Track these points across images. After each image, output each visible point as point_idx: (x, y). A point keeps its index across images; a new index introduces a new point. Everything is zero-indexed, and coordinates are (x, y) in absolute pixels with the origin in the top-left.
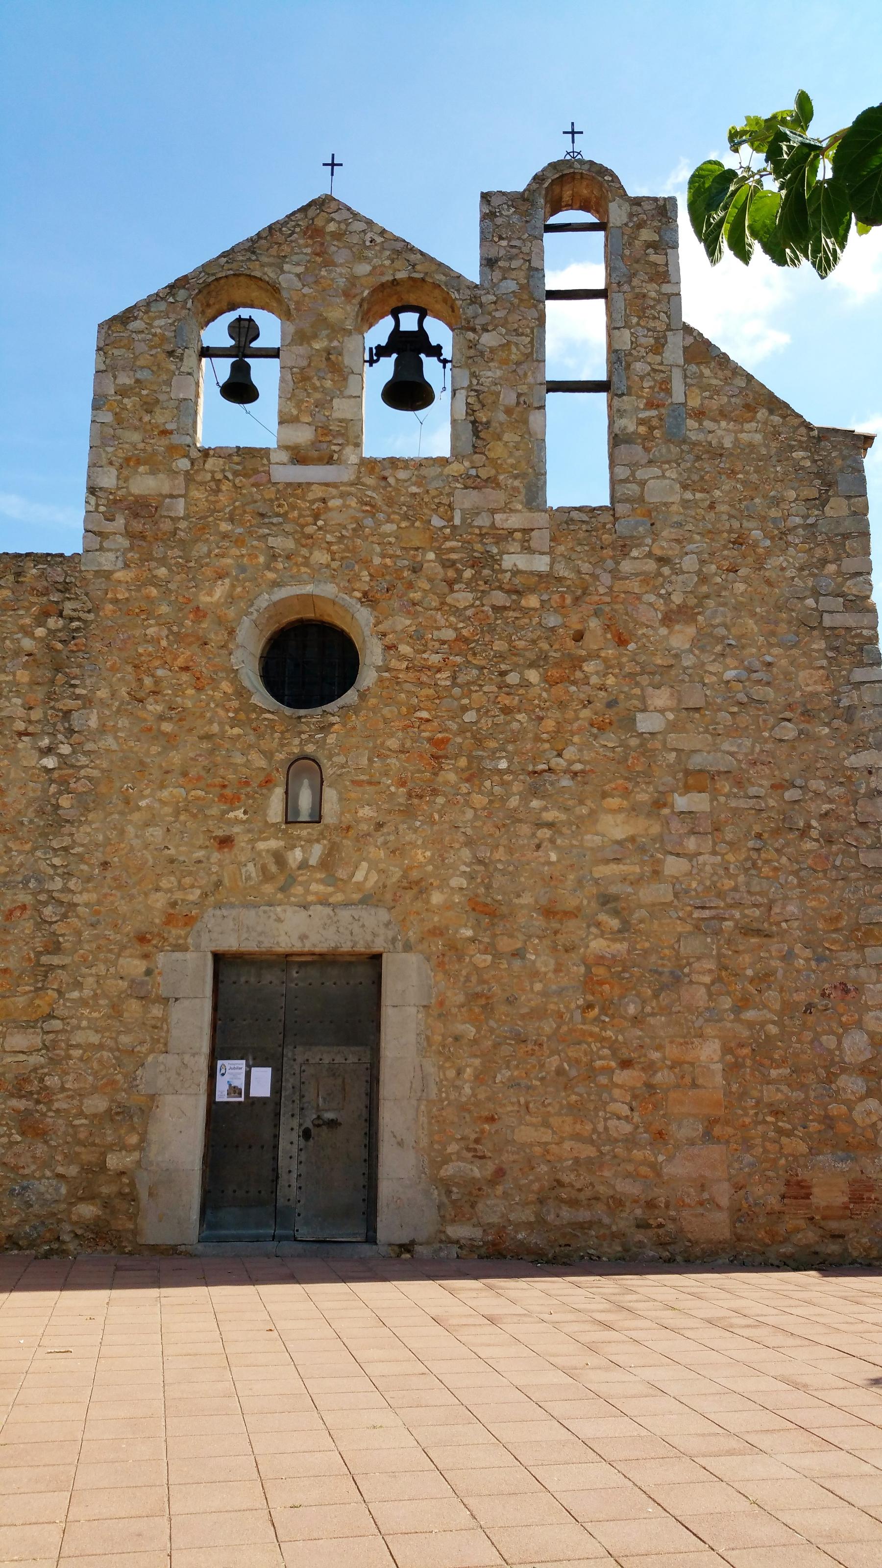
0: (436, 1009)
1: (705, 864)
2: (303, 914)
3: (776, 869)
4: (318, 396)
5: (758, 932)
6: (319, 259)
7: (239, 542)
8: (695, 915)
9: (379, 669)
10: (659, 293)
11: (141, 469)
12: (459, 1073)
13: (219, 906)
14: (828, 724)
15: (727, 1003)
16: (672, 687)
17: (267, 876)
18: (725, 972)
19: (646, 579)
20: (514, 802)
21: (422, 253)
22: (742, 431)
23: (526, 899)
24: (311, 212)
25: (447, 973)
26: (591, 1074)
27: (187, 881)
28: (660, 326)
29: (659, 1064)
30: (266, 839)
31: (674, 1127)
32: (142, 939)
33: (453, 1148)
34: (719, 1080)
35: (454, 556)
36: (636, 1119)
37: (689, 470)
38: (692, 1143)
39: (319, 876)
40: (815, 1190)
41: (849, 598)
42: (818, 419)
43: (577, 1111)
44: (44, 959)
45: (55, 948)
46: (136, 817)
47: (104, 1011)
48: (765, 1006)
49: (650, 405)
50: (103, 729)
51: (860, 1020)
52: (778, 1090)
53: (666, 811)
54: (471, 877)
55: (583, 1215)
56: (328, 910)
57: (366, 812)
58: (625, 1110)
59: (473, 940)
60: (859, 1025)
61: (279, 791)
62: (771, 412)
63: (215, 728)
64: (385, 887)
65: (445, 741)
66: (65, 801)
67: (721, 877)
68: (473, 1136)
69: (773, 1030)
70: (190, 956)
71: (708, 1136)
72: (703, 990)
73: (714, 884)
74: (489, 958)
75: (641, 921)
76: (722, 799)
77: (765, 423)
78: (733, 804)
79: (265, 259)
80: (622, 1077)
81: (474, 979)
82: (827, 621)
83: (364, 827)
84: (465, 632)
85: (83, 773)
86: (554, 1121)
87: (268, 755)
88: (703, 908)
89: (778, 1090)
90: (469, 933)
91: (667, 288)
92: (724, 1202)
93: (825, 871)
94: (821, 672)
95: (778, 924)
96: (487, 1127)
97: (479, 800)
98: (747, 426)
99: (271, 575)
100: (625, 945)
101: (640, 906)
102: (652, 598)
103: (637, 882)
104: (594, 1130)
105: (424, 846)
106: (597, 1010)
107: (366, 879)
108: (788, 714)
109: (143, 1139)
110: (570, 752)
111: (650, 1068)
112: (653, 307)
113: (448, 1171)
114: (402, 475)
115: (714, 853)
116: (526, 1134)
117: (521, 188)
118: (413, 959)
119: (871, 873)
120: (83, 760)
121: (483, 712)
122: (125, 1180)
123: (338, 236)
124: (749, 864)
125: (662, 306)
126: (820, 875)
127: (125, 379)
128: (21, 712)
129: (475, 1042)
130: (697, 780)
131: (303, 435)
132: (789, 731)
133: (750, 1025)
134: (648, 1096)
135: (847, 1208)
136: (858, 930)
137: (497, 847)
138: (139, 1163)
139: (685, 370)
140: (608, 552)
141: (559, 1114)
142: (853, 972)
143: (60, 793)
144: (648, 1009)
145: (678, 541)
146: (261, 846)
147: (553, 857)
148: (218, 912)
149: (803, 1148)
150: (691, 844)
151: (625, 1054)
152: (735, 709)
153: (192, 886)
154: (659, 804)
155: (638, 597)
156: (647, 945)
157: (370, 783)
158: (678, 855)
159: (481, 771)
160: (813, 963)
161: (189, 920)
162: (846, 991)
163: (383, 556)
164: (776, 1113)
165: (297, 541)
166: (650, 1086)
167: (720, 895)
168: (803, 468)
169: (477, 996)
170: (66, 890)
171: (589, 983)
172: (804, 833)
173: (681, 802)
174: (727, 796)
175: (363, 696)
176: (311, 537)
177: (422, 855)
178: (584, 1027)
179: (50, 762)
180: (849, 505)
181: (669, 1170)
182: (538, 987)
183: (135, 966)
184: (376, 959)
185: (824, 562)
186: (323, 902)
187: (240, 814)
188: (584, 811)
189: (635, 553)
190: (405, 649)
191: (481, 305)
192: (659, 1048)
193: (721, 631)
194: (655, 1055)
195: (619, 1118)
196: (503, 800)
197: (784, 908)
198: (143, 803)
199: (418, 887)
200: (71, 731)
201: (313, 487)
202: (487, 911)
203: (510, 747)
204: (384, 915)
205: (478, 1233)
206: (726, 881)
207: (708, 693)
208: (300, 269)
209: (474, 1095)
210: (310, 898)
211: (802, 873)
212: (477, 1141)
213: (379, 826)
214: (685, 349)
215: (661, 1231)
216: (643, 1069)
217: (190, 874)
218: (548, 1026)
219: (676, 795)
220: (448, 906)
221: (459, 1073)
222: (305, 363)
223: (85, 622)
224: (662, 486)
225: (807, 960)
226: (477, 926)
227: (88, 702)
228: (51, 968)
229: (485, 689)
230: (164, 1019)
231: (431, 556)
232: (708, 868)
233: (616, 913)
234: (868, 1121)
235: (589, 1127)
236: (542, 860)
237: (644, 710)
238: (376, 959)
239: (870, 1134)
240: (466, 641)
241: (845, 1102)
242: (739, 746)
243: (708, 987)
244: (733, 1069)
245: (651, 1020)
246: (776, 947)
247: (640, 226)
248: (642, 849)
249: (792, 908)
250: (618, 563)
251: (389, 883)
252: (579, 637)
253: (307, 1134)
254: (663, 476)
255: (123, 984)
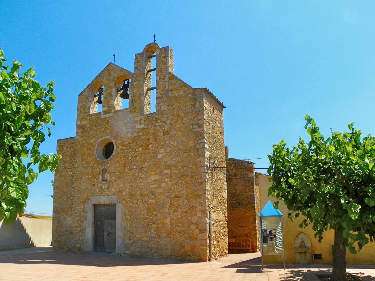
0: (124, 214)
1: (168, 184)
2: (104, 197)
3: (182, 184)
4: (108, 101)
5: (178, 197)
6: (109, 75)
7: (96, 131)
8: (167, 194)
9: (116, 151)
10: (165, 67)
11: (83, 120)
12: (127, 225)
13: (93, 196)
14: (193, 153)
15: (172, 211)
16: (164, 148)
17: (99, 191)
18: (172, 205)
19: (161, 126)
20: (136, 174)
21: (125, 69)
22: (180, 92)
23: (138, 193)
24: (108, 66)
25: (125, 207)
26: (148, 225)
27: (89, 192)
28: (165, 74)
29: (159, 223)
30: (99, 184)
31: (162, 235)
32: (83, 202)
33: (126, 238)
34: (170, 226)
35: (128, 127)
36: (155, 233)
37: (169, 103)
38: (165, 238)
39: (107, 190)
40: (185, 247)
41: (199, 125)
42: (194, 85)
43: (146, 232)
44: (72, 206)
45: (73, 204)
46: (82, 181)
47: (79, 214)
48: (178, 212)
49: (162, 90)
50: (78, 167)
51: (196, 214)
52: (180, 228)
53: (162, 174)
54: (129, 189)
55: (146, 250)
56: (108, 196)
57: (114, 178)
58: (153, 232)
59: (129, 201)
60: (196, 215)
61: (101, 175)
62: (185, 87)
63: (92, 165)
64: (116, 192)
65: (126, 163)
66: (73, 179)
67: (171, 186)
68: (129, 236)
69: (179, 216)
70: (89, 205)
71: (167, 237)
72: (167, 209)
73: (170, 188)
74: (132, 204)
75: (157, 196)
76: (172, 171)
77: (184, 90)
78: (174, 171)
79: (101, 77)
80: (153, 226)
81: (130, 208)
82: (194, 130)
83: (113, 181)
84: (129, 142)
85: (75, 175)
86: (142, 234)
87: (100, 169)
88: (168, 193)
89: (180, 228)
90: (129, 200)
91: (166, 66)
92: (170, 249)
93: (191, 184)
94: (193, 141)
95: (182, 195)
96: (131, 234)
97: (131, 174)
98: (180, 91)
99: (100, 136)
100: (154, 201)
101: (157, 193)
102: (161, 130)
103: (156, 188)
104: (149, 235)
105: (122, 184)
106: (149, 213)
107: (113, 191)
108: (186, 151)
109: (84, 235)
110: (146, 164)
111: (158, 224)
112: (163, 70)
113: (125, 242)
114: (120, 113)
115: (170, 182)
116: (137, 236)
117: (141, 52)
118: (120, 205)
119: (199, 183)
120: (75, 172)
121: (132, 157)
122: (82, 241)
123: (112, 70)
124: (176, 184)
125: (165, 70)
126: (190, 185)
127: (81, 105)
128: (68, 165)
129: (130, 220)
130: (168, 167)
131: (106, 109)
132: (186, 155)
133: (176, 215)
134: (158, 229)
135: (191, 250)
136: (196, 195)
137: (134, 183)
138: (84, 238)
139: (169, 82)
140: (154, 122)
141: (143, 232)
142: (195, 204)
143: (73, 178)
144: (158, 213)
145: (167, 118)
146: (99, 185)
147: (143, 184)
148: (93, 197)
149: (184, 239)
150: (166, 180)
151: (154, 221)
152: (175, 151)
153: (89, 193)
154: (161, 172)
155: (159, 130)
156: (158, 201)
157: (114, 172)
158: (164, 183)
159: (131, 168)
160: (187, 203)
161: (89, 199)
162: (193, 208)
163: (117, 129)
164: (179, 232)
165: (105, 129)
166: (158, 227)
167: (171, 190)
168: (191, 98)
169: (130, 211)
170: (74, 194)
171: (148, 208)
172: (187, 176)
173: (165, 172)
174: (173, 170)
175: (113, 156)
176: (106, 127)
177: (122, 186)
178: (147, 217)
179: (71, 173)
180: (200, 104)
181: (160, 242)
182: (140, 209)
183: (82, 207)
184: (115, 205)
185: (194, 117)
186: (107, 195)
187: (96, 180)
188: (148, 175)
189: (158, 121)
190: (120, 147)
191: (134, 77)
192: (159, 220)
193: (174, 135)
194: (159, 222)
195: (153, 233)
196: (135, 174)
197: (183, 192)
198: (83, 179)
199: (121, 191)
200: (74, 168)
201: (107, 118)
202: (131, 195)
203: (136, 164)
204: (116, 197)
205: (130, 252)
206: (172, 187)
207: (171, 148)
208: (106, 78)
209: (130, 229)
210: (106, 194)
211: (187, 185)
212: (130, 237)
213: (116, 180)
214: (169, 77)
215: (159, 253)
216: (157, 224)
217: (89, 191)
218: (141, 216)
219: (164, 170)
220: (126, 195)
221: (127, 225)
222: (106, 95)
223: (76, 148)
224: (164, 107)
225: (186, 202)
226: (130, 199)
227: (76, 162)
228: (72, 207)
229: (133, 152)
230: (86, 215)
231: (124, 128)
232: (169, 185)
233: (153, 195)
234: (196, 234)
235: (148, 235)
236: (141, 185)
237: (159, 154)
238: (115, 205)
239: (196, 236)
240: (130, 143)
241: (192, 230)
242: (176, 159)
243: (168, 208)
244: (172, 224)
245: (158, 215)
246: (181, 200)
247: (162, 54)
248: (158, 182)
249: (184, 192)
250: (156, 124)
251: (117, 191)
252: (148, 140)
253: (108, 235)
254: (164, 105)
255: (81, 210)
